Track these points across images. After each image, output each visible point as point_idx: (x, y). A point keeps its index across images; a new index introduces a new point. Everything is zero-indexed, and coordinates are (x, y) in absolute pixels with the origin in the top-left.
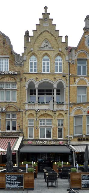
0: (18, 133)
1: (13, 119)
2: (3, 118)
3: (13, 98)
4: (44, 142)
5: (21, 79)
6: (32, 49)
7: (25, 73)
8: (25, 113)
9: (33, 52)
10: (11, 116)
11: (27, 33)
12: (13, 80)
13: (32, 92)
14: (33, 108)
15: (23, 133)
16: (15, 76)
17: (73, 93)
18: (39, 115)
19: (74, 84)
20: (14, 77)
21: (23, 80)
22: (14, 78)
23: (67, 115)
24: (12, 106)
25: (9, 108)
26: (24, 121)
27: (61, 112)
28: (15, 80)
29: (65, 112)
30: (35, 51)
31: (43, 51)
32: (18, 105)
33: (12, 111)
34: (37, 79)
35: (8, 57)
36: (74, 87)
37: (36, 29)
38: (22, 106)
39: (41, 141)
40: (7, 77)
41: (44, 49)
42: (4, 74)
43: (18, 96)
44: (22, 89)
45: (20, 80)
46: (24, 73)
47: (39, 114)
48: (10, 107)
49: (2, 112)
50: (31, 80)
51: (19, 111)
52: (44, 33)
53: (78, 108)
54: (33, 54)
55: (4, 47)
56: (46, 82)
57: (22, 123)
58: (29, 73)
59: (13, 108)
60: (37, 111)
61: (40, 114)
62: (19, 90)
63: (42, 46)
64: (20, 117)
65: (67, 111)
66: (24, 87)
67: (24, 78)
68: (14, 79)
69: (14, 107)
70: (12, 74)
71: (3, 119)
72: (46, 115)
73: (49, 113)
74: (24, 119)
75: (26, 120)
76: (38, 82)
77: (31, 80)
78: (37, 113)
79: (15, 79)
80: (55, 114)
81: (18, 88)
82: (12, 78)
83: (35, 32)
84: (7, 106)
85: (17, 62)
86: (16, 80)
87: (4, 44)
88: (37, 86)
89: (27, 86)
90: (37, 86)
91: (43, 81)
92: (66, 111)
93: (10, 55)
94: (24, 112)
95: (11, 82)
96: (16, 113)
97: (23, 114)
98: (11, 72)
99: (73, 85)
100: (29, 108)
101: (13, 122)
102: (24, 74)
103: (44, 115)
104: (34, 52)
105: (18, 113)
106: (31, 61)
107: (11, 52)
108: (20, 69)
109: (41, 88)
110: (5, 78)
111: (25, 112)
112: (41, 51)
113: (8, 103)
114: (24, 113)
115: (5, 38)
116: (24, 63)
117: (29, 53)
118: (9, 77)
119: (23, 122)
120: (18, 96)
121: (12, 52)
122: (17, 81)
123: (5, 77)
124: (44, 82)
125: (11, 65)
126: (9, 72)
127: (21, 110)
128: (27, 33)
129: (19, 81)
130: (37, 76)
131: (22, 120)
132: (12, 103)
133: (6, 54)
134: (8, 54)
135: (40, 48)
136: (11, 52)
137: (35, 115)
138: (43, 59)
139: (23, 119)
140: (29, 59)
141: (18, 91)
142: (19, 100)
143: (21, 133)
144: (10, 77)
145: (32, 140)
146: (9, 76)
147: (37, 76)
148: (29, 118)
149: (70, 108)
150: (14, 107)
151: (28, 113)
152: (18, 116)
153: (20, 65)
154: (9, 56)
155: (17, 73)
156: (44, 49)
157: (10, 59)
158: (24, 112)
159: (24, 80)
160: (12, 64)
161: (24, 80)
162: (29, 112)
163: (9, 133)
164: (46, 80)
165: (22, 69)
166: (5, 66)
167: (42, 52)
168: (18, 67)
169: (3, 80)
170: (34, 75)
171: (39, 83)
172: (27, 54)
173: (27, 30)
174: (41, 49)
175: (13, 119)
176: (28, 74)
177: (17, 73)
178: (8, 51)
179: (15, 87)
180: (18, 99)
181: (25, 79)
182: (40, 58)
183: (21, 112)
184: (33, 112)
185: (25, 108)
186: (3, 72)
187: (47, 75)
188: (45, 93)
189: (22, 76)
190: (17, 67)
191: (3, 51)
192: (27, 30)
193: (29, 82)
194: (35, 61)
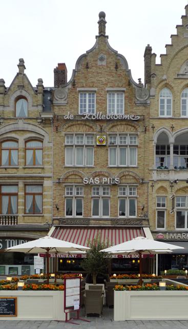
0: (141, 220)
1: (131, 196)
2: (115, 194)
3: (131, 159)
4: (184, 235)
6: (165, 77)
8: (152, 186)
9: (165, 82)
10: (127, 191)
11: (148, 50)
13: (162, 150)
14: (166, 178)
15: (148, 220)
16: (136, 123)
18: (176, 189)
20: (133, 124)
21: (149, 130)
22: (133, 126)
24: (130, 174)
25: (124, 178)
26: (150, 199)
30: (170, 81)
31: (182, 80)
33: (130, 182)
34: (172, 128)
35: (124, 91)
37: (170, 43)
38: (147, 175)
39: (179, 234)
40: (121, 125)
41: (185, 77)
42: (118, 120)
43: (140, 156)
44: (147, 145)
45: (144, 130)
47: (176, 187)
48: (126, 175)
49: (113, 185)
50: (164, 129)
51: (143, 183)
52: (185, 50)
54: (167, 86)
55: (116, 73)
57: (147, 203)
58: (159, 117)
59: (131, 178)
60: (172, 183)
61: (178, 188)
62: (142, 146)
63: (181, 72)
64: (144, 193)
66: (150, 142)
67: (150, 127)
69: (133, 177)
70: (130, 120)
71: (114, 196)
75: (153, 198)
76: (174, 132)
77: (164, 129)
78: (173, 186)
79: (135, 127)
81: (140, 144)
82: (130, 127)
83: (169, 47)
84: (122, 175)
85: (138, 99)
86: (136, 129)
87: (116, 68)
88: (172, 140)
89: (155, 141)
90: (172, 140)
91: (183, 131)
93: (128, 87)
94: (150, 184)
95: (129, 133)
96: (137, 186)
97: (148, 187)
98: (128, 116)
100: (159, 178)
101: (130, 201)
102: (151, 120)
104: (169, 82)
105: (139, 186)
106: (162, 98)
107: (129, 82)
108: (144, 110)
109: (180, 144)
110: (119, 127)
111: (152, 184)
112: (180, 81)
113: (123, 170)
115: (119, 58)
116: (152, 100)
117: (159, 83)
118: (126, 124)
119: (148, 201)
120: (140, 156)
121: (130, 82)
123: (117, 125)
124: (183, 134)
125: (129, 104)
126: (126, 117)
127: (146, 180)
128: (148, 50)
129: (142, 132)
130: (173, 123)
131: (147, 198)
132: (131, 170)
133: (120, 85)
134: (124, 86)
135: (178, 75)
136: (129, 82)
137: (169, 189)
138: (183, 94)
139: (148, 196)
140: (159, 93)
141: (140, 148)
142: (142, 164)
143: (145, 220)
144: (127, 125)
145: (165, 233)
146: (124, 123)
147: (173, 123)
148: (158, 194)
150: (134, 175)
151: (157, 186)
152: (140, 191)
153: (145, 105)
154: (125, 89)
155: (139, 117)
156: (185, 77)
157: (127, 94)
158: (150, 184)
160: (130, 103)
161: (151, 130)
162: (158, 183)
163: (125, 220)
165: (146, 110)
166: (118, 105)
167: (182, 82)
168: (141, 107)
169: (115, 129)
170: (168, 120)
171: (176, 134)
172: (156, 84)
173: (148, 45)
174: (179, 77)
175: (131, 196)
176: (157, 120)
177: (139, 117)
178: (124, 81)
179: (135, 142)
180: (139, 162)
181: (153, 127)
182: (178, 91)
183: (146, 185)
184: (166, 185)
185: (152, 178)
186: (116, 117)
188: (179, 150)
189: (147, 123)
191: (116, 81)
192: (148, 45)
193: (159, 132)
194: (169, 98)
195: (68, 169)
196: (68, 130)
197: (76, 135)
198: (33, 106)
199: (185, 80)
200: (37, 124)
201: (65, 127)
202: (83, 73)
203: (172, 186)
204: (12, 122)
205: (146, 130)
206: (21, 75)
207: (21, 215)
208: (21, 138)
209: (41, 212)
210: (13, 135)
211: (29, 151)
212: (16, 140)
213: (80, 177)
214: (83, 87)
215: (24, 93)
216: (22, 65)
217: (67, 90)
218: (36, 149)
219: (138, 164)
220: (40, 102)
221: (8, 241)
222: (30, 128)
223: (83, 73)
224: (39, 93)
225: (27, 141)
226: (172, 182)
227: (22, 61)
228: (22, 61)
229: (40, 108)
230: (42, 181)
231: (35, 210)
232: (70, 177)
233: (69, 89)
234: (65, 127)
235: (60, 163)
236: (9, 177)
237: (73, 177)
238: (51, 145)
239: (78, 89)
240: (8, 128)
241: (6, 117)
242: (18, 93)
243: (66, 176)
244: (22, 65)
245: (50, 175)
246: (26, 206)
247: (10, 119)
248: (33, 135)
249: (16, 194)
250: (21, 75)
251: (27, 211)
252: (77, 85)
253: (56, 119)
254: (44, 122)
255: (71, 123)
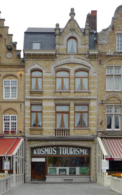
195: (108, 93)
196: (109, 63)
197: (115, 67)
198: (82, 45)
200: (85, 58)
201: (107, 61)
202: (120, 20)
204: (65, 57)
206: (72, 21)
207: (72, 128)
208: (72, 69)
209: (87, 126)
210: (66, 67)
211: (78, 79)
212: (68, 71)
213: (118, 99)
214: (120, 30)
215: (75, 35)
216: (72, 13)
217: (108, 33)
218: (83, 78)
220: (87, 42)
221: (61, 148)
222: (80, 61)
223: (120, 20)
224: (87, 35)
225: (76, 71)
227: (72, 10)
228: (72, 10)
229: (87, 46)
230: (89, 102)
231: (81, 124)
232: (110, 99)
233: (109, 32)
234: (107, 61)
235: (103, 88)
236: (63, 99)
237: (113, 99)
238: (96, 74)
239: (116, 32)
240: (62, 62)
241: (61, 53)
242: (70, 35)
243: (107, 98)
244: (72, 13)
245: (96, 97)
246: (76, 121)
247: (64, 54)
248: (82, 67)
249: (68, 113)
250: (72, 21)
251: (76, 126)
252: (115, 29)
253: (100, 55)
254: (91, 57)
255: (111, 58)
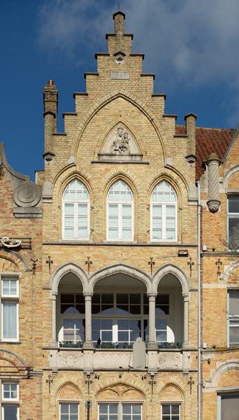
5: (35, 265)
6: (71, 160)
7: (49, 241)
8: (49, 382)
12: (6, 266)
17: (216, 312)
18: (98, 389)
19: (216, 281)
21: (41, 267)
22: (9, 260)
23: (194, 387)
26: (45, 407)
27: (174, 378)
28: (12, 268)
29: (187, 379)
30: (84, 167)
32: (24, 354)
34: (89, 263)
36: (217, 290)
41: (114, 159)
43: (24, 321)
45: (30, 268)
46: (44, 241)
47: (98, 384)
52: (113, 103)
53: (230, 366)
54: (78, 177)
56: (120, 274)
59: (7, 364)
61: (102, 386)
63: (107, 149)
64: (33, 396)
65: (195, 376)
67: (44, 261)
68: (10, 262)
72: (121, 388)
73: (132, 383)
74: (45, 401)
75: (51, 406)
76: (91, 273)
78: (91, 382)
79: (13, 262)
80: (153, 383)
88: (88, 289)
89: (55, 289)
90: (88, 289)
91: (111, 270)
92: (190, 374)
94: (46, 376)
99: (213, 286)
103: (114, 388)
108: (31, 227)
114: (44, 381)
116: (46, 206)
120: (24, 321)
122: (22, 271)
129: (27, 271)
130: (91, 252)
135: (99, 155)
137: (84, 389)
141: (23, 303)
142: (27, 337)
149: (206, 365)
150: (12, 358)
152: (27, 392)
156: (114, 159)
159: (44, 268)
161: (45, 267)
162: (61, 376)
164: (122, 268)
165: (36, 227)
167: (107, 170)
168: (24, 221)
172: (54, 175)
174: (102, 159)
177: (20, 241)
180: (23, 333)
181: (49, 262)
182: (100, 190)
183: (36, 379)
184: (77, 378)
187: (125, 248)
189: (37, 254)
190: (18, 222)
199: (112, 165)
203: (89, 383)
205: (34, 268)
219: (20, 336)
226: (89, 373)
